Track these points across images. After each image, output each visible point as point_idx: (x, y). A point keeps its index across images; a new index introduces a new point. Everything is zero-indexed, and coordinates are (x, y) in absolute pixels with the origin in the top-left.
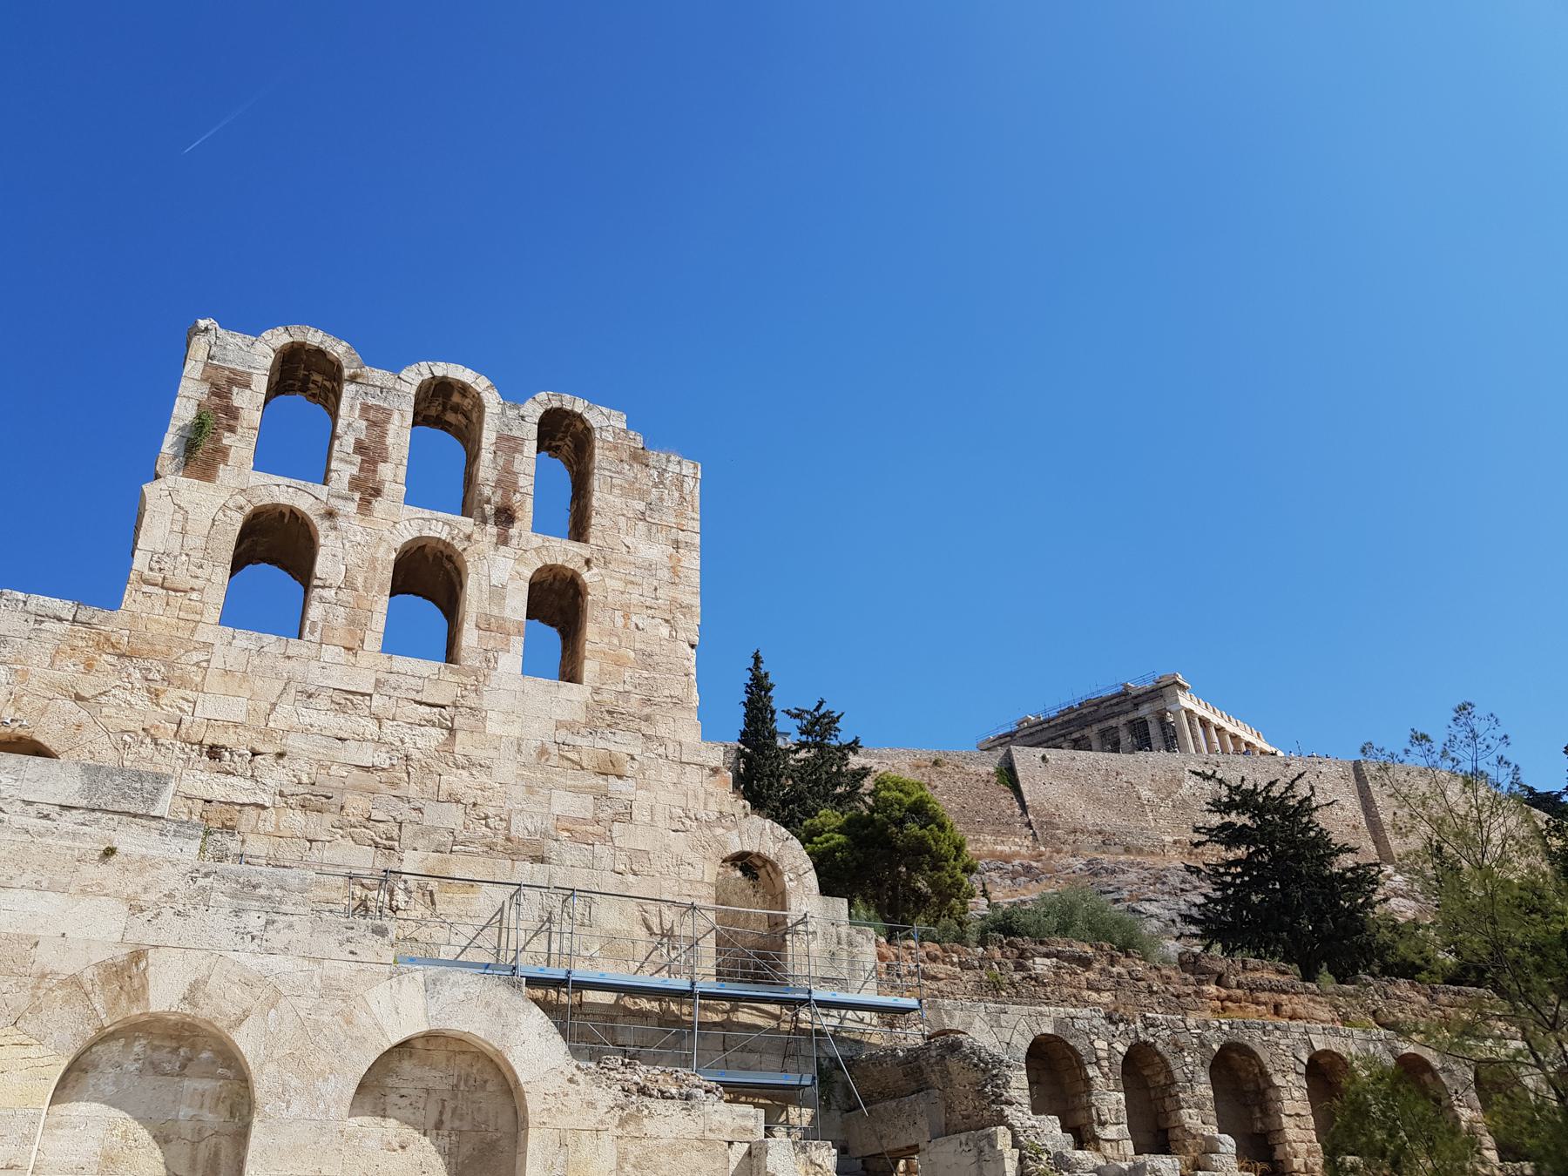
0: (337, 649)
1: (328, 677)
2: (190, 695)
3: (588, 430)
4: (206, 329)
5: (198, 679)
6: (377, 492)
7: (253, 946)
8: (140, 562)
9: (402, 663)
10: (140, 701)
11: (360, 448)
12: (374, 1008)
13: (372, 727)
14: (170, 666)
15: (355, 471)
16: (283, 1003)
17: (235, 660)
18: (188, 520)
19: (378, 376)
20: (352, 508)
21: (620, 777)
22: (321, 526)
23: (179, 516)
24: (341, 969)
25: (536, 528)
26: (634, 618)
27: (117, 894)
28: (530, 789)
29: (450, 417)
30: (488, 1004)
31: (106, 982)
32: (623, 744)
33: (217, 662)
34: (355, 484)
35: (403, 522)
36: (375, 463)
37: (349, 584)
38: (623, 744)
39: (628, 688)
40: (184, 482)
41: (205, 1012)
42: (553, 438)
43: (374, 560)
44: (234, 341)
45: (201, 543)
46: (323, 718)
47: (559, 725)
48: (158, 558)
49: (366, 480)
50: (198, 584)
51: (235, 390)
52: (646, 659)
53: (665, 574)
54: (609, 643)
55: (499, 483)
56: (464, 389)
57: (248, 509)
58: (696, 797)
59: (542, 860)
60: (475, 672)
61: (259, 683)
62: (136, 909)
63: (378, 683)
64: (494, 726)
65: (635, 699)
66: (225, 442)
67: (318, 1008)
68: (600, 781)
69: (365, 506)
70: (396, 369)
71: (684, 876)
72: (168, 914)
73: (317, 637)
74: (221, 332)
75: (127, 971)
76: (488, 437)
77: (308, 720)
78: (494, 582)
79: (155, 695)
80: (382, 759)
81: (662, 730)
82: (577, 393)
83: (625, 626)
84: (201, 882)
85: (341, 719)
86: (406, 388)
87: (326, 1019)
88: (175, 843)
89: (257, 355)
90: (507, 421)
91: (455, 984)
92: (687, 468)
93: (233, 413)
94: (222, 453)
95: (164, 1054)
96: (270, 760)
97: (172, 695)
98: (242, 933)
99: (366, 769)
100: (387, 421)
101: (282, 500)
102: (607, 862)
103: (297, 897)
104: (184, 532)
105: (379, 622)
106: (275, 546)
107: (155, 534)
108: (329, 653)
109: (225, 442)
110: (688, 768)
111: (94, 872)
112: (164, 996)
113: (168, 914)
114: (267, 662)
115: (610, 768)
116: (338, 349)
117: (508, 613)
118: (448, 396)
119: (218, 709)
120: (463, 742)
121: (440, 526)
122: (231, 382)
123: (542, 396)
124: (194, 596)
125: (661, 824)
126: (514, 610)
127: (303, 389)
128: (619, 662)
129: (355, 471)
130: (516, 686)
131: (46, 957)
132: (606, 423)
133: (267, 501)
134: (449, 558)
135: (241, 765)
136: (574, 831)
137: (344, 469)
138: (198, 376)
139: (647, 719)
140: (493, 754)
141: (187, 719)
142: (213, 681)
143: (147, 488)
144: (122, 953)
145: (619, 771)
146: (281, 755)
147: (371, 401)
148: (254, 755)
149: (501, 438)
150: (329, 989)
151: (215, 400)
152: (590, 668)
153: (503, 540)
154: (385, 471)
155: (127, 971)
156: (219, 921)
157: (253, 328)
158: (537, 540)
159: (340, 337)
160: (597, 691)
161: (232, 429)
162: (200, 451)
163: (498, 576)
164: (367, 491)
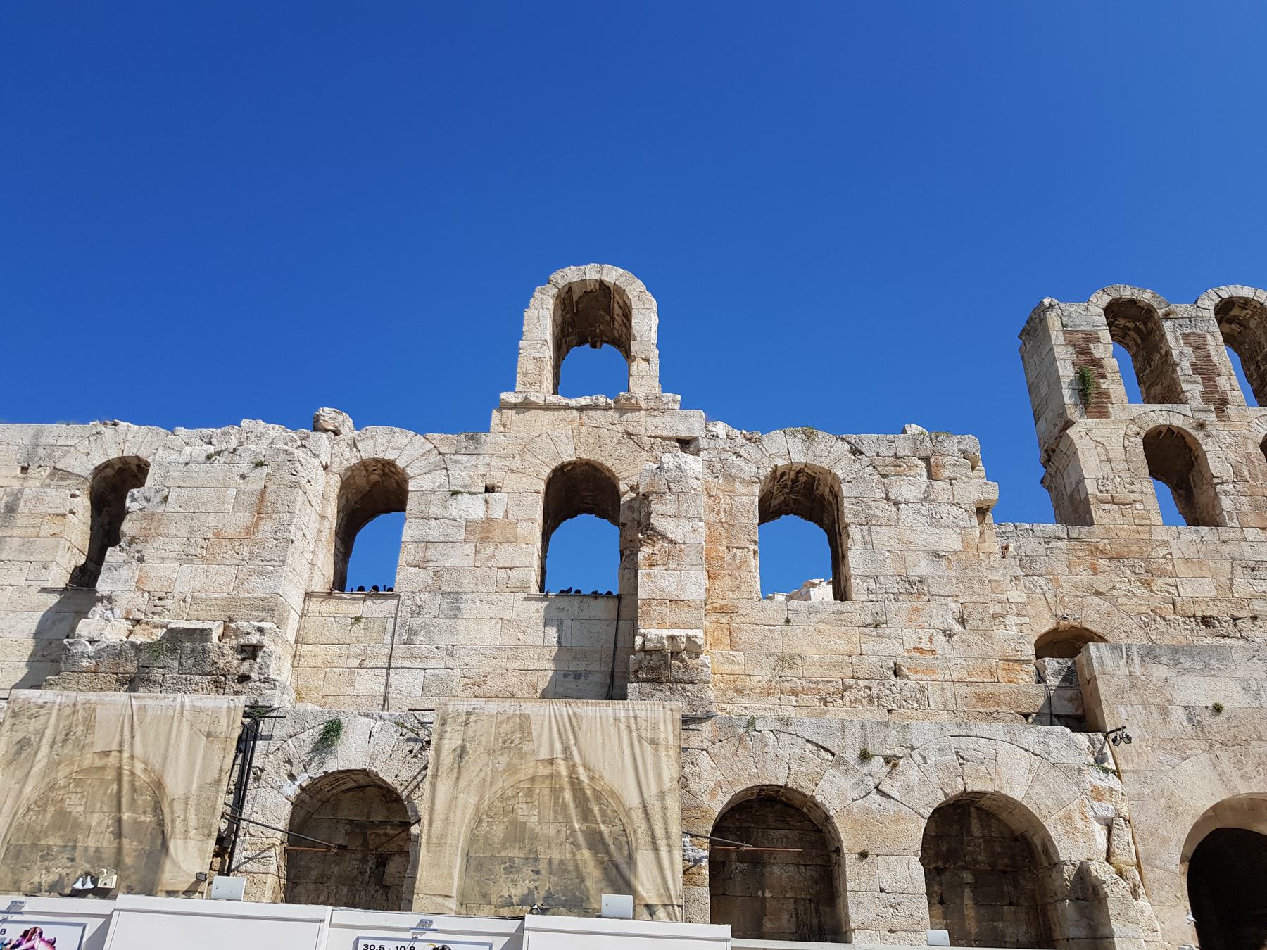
0: (1255, 531)
1: (1258, 553)
2: (1171, 581)
4: (1051, 306)
5: (1170, 568)
10: (1141, 591)
11: (1197, 369)
14: (1147, 561)
15: (1201, 388)
17: (1190, 551)
20: (1212, 418)
22: (1199, 436)
23: (1100, 449)
34: (1207, 398)
36: (1213, 379)
37: (1239, 478)
40: (1092, 423)
43: (1248, 455)
44: (1074, 309)
45: (1124, 466)
48: (1101, 482)
49: (1212, 393)
50: (1137, 496)
51: (1092, 346)
57: (1143, 434)
61: (1213, 565)
66: (1104, 386)
69: (1221, 414)
73: (1236, 523)
74: (1062, 305)
77: (1261, 589)
79: (1147, 585)
93: (1097, 363)
94: (1104, 395)
96: (1249, 623)
97: (1158, 583)
100: (1205, 344)
101: (1162, 421)
104: (1109, 460)
106: (1173, 460)
109: (1104, 386)
114: (1212, 548)
119: (1196, 588)
122: (1086, 340)
124: (1138, 506)
133: (1152, 425)
135: (1230, 629)
137: (1193, 389)
138: (1063, 342)
141: (1178, 599)
142: (1181, 568)
146: (1255, 618)
147: (1188, 331)
148: (1235, 619)
151: (1082, 357)
154: (1222, 382)
159: (1144, 287)
161: (1103, 376)
162: (1091, 397)
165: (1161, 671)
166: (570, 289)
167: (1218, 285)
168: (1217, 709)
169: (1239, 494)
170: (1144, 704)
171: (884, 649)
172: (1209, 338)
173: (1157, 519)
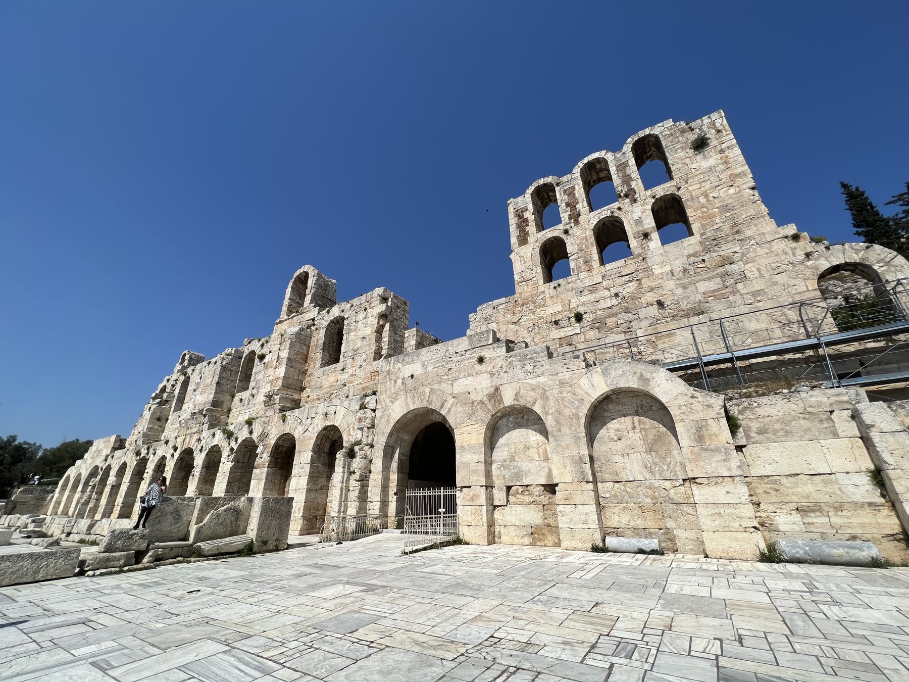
3: (656, 138)
6: (579, 215)
7: (532, 376)
8: (516, 277)
9: (608, 266)
10: (531, 317)
11: (568, 205)
12: (583, 386)
13: (607, 293)
14: (534, 303)
16: (547, 393)
18: (525, 259)
19: (565, 178)
20: (572, 225)
21: (731, 264)
24: (565, 375)
25: (647, 188)
26: (711, 195)
27: (486, 372)
28: (685, 288)
29: (602, 175)
30: (635, 373)
31: (490, 400)
32: (727, 250)
33: (547, 295)
34: (570, 217)
35: (591, 219)
38: (727, 250)
39: (719, 225)
40: (520, 249)
41: (522, 402)
42: (646, 153)
46: (588, 298)
47: (689, 256)
52: (726, 208)
53: (722, 167)
54: (702, 212)
55: (623, 183)
56: (598, 160)
58: (786, 253)
59: (702, 313)
60: (640, 255)
62: (492, 375)
63: (603, 277)
64: (657, 270)
65: (726, 228)
67: (561, 392)
68: (722, 270)
69: (577, 222)
70: (570, 171)
71: (793, 292)
72: (502, 373)
75: (495, 394)
76: (613, 169)
78: (635, 218)
81: (748, 233)
82: (643, 128)
83: (708, 200)
84: (509, 360)
85: (594, 295)
86: (576, 175)
87: (565, 395)
88: (498, 350)
89: (525, 201)
90: (620, 160)
91: (616, 369)
92: (715, 116)
93: (526, 221)
94: (528, 233)
95: (519, 420)
97: (538, 310)
98: (528, 373)
99: (610, 308)
102: (739, 301)
103: (542, 354)
105: (595, 256)
107: (517, 267)
108: (582, 275)
110: (773, 243)
111: (478, 367)
112: (508, 400)
113: (502, 373)
116: (549, 179)
117: (646, 226)
118: (595, 167)
119: (553, 309)
120: (646, 283)
121: (604, 212)
122: (522, 212)
123: (630, 139)
125: (767, 275)
126: (649, 224)
127: (551, 201)
128: (711, 217)
129: (569, 213)
130: (661, 251)
131: (473, 397)
132: (662, 129)
134: (616, 221)
136: (716, 294)
137: (565, 216)
139: (737, 232)
140: (660, 281)
142: (549, 302)
143: (512, 256)
144: (492, 390)
145: (732, 261)
149: (617, 167)
150: (562, 383)
152: (695, 227)
153: (635, 201)
154: (579, 206)
155: (495, 394)
156: (518, 371)
157: (522, 192)
158: (649, 193)
159: (548, 176)
160: (702, 235)
161: (527, 225)
163: (637, 215)
164: (575, 217)
165: (399, 365)
166: (298, 277)
167: (582, 158)
168: (412, 376)
169: (580, 257)
170: (390, 380)
171: (345, 377)
172: (576, 187)
173: (541, 281)
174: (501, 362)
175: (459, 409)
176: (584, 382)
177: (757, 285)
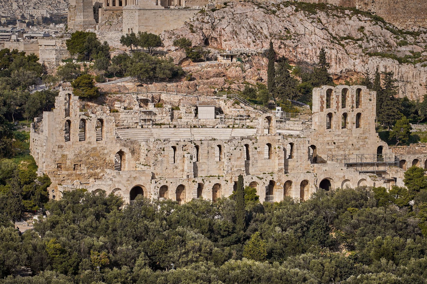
10: (322, 139)
11: (336, 102)
24: (356, 175)
26: (368, 118)
32: (367, 135)
35: (342, 111)
64: (354, 135)
80: (343, 141)
115: (366, 138)
142: (327, 135)
149: (352, 95)
155: (344, 177)
174: (345, 171)
175: (337, 179)
176: (358, 177)
177: (369, 146)
